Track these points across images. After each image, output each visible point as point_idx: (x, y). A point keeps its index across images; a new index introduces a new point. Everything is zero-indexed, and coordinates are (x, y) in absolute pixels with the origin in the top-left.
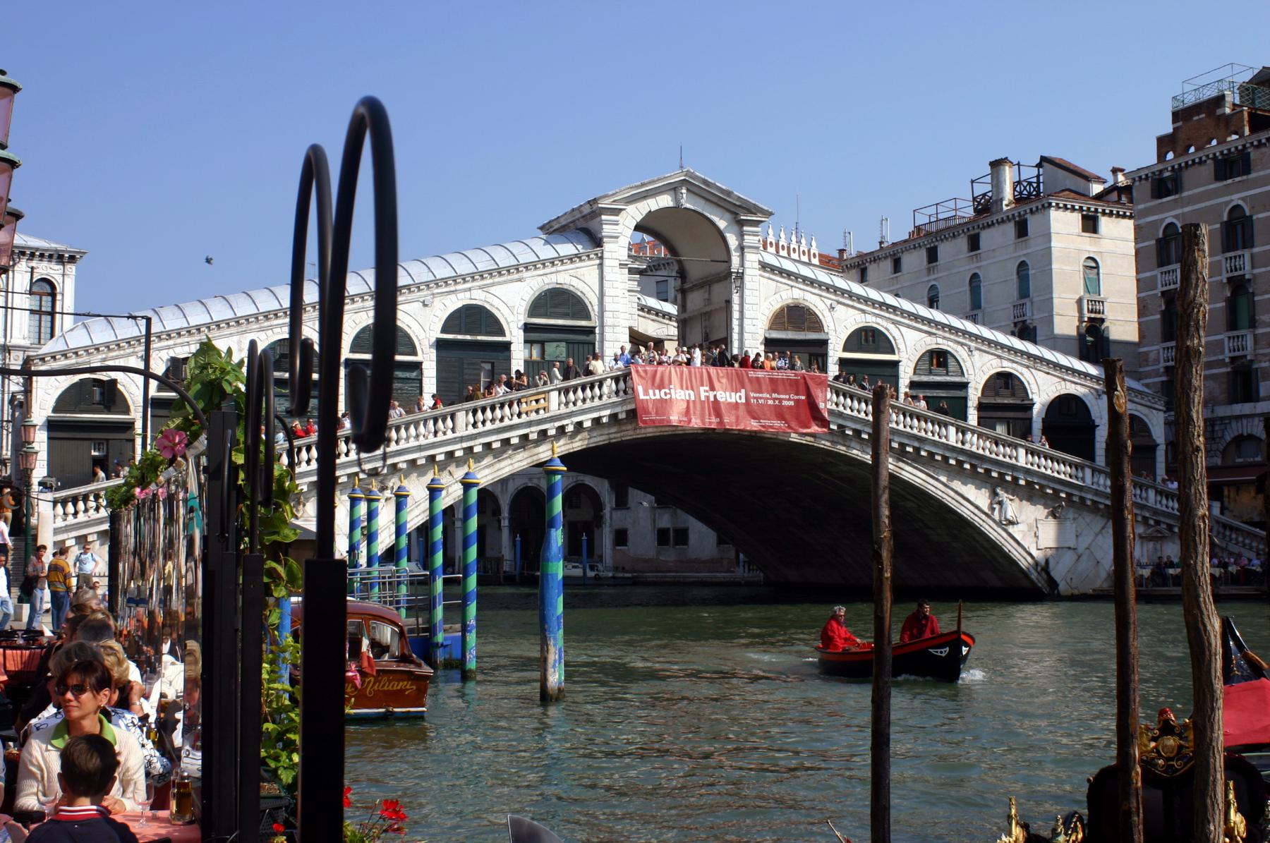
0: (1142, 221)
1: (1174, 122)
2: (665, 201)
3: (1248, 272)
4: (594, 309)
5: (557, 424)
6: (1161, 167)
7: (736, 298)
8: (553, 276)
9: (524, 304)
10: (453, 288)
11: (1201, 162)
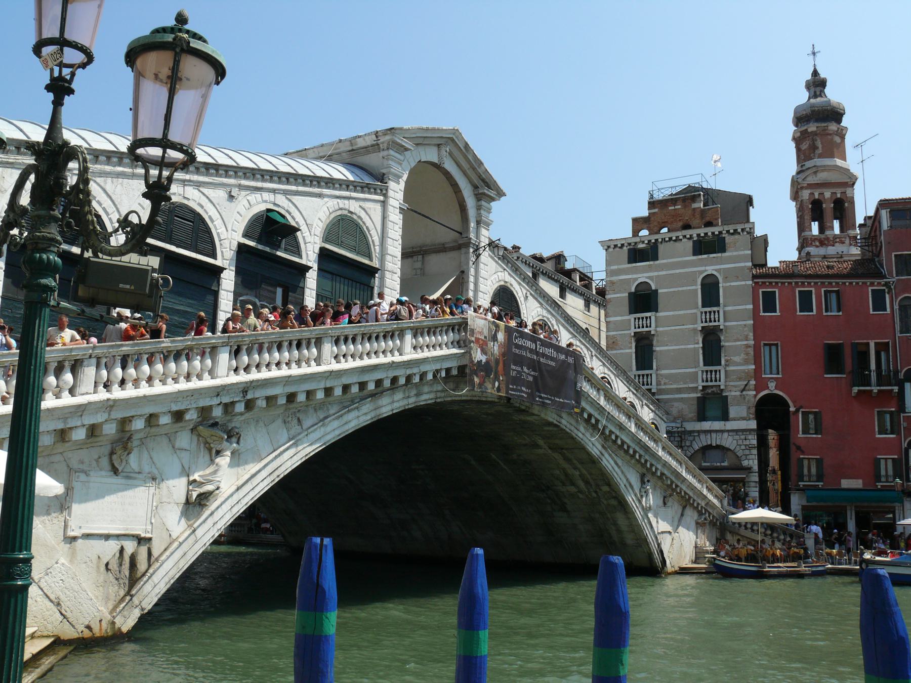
0: (614, 278)
1: (649, 208)
2: (431, 155)
3: (721, 324)
4: (376, 250)
5: (409, 372)
6: (637, 239)
7: (472, 271)
8: (346, 202)
9: (321, 225)
10: (259, 184)
11: (677, 239)
